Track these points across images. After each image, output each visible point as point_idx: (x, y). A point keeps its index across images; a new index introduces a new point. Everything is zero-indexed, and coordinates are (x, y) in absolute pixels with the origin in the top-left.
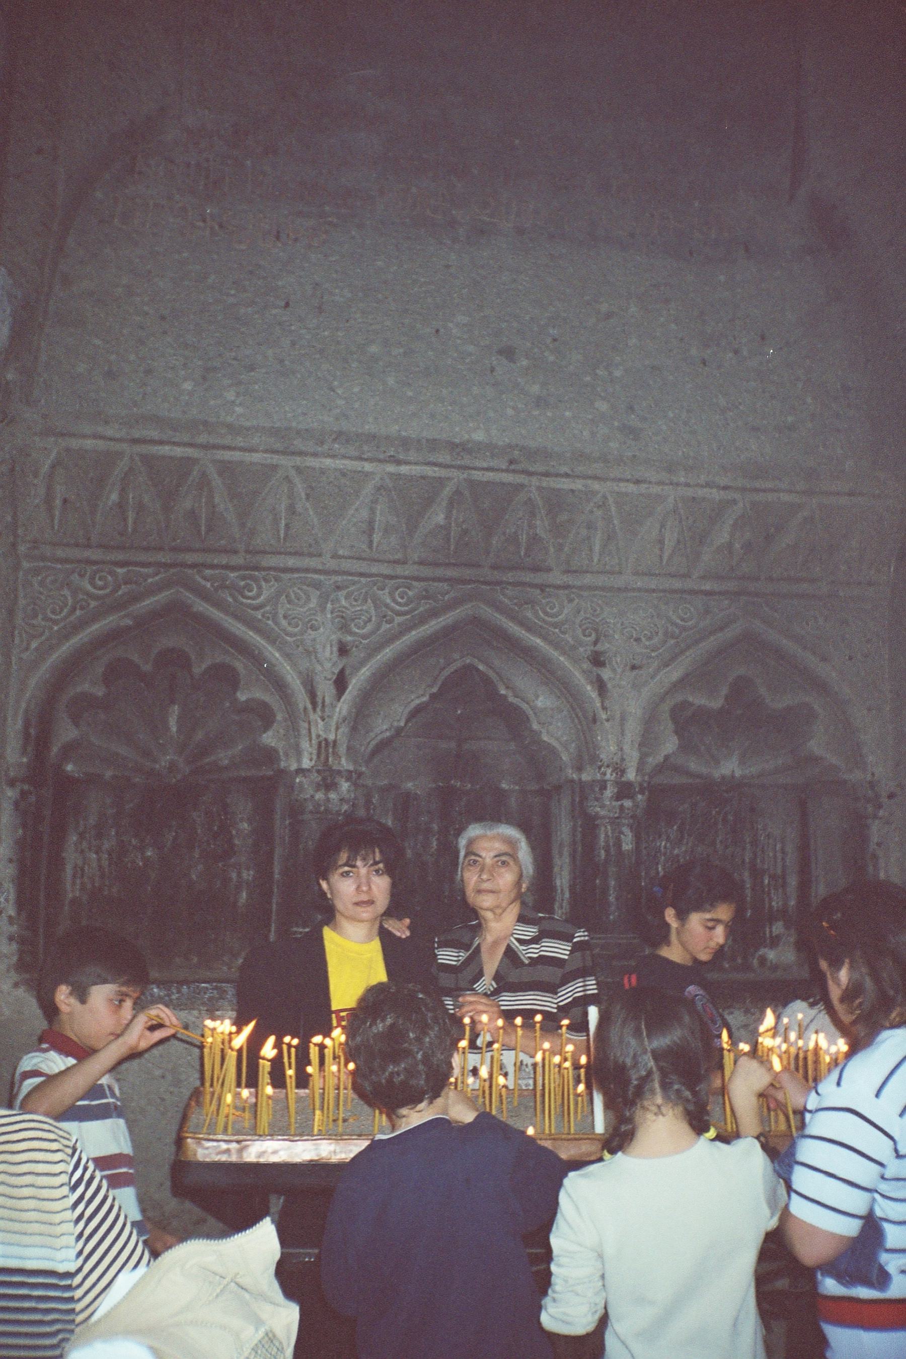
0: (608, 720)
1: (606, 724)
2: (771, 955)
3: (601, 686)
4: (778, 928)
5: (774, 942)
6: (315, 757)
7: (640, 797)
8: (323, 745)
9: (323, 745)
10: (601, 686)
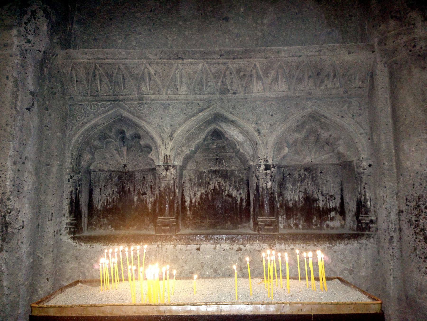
2: (331, 224)
4: (333, 214)
5: (332, 219)
7: (273, 169)
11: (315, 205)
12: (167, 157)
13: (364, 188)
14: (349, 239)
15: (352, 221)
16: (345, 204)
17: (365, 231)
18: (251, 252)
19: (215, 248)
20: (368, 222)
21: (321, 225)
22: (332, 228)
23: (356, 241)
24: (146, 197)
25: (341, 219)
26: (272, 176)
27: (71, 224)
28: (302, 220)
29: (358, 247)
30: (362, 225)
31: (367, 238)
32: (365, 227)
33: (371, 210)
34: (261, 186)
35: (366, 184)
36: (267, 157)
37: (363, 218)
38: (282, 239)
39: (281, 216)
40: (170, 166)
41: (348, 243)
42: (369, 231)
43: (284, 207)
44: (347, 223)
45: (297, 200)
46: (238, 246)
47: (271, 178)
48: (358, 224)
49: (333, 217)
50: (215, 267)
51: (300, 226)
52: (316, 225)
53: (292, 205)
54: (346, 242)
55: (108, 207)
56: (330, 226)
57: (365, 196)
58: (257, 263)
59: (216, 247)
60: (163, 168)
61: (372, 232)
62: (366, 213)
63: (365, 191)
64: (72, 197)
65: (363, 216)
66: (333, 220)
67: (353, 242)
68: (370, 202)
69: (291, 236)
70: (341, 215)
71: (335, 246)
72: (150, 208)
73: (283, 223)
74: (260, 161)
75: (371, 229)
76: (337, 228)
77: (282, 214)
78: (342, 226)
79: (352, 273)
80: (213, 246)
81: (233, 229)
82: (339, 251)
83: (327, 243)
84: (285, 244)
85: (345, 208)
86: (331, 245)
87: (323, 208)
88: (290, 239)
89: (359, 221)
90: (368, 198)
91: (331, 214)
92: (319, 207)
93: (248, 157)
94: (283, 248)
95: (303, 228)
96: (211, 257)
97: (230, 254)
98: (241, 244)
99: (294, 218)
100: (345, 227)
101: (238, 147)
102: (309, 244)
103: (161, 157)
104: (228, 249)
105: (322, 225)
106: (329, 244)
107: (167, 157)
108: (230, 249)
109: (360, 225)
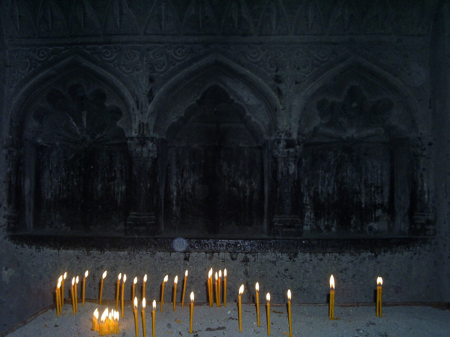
0: (283, 110)
1: (282, 111)
2: (375, 226)
3: (279, 92)
4: (379, 212)
5: (377, 220)
6: (137, 131)
7: (298, 147)
8: (142, 126)
9: (142, 126)
10: (279, 92)
12: (143, 126)
13: (422, 176)
24: (114, 184)
26: (296, 157)
27: (9, 218)
33: (429, 206)
34: (280, 171)
35: (424, 169)
36: (290, 129)
40: (147, 138)
45: (331, 192)
47: (294, 159)
49: (379, 217)
51: (333, 229)
52: (355, 228)
53: (323, 200)
55: (61, 196)
57: (423, 186)
60: (137, 141)
63: (422, 180)
64: (11, 181)
68: (429, 195)
72: (119, 201)
73: (310, 225)
74: (280, 134)
90: (425, 189)
91: (376, 213)
93: (263, 129)
101: (248, 114)
103: (135, 126)
107: (143, 126)
109: (413, 226)
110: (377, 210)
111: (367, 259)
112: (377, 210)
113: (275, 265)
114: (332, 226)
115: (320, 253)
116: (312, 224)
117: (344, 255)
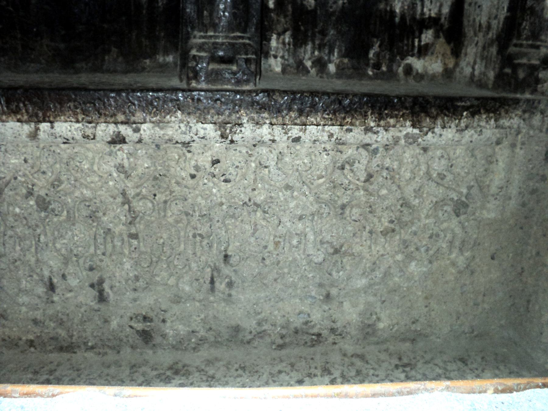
2: (418, 64)
4: (427, 36)
5: (423, 51)
11: (382, 6)
14: (474, 112)
15: (482, 58)
16: (466, 6)
17: (523, 92)
18: (158, 146)
19: (34, 136)
20: (535, 62)
21: (390, 69)
22: (420, 77)
23: (492, 122)
25: (449, 52)
28: (340, 51)
29: (494, 139)
30: (515, 71)
31: (524, 112)
32: (524, 79)
37: (524, 50)
38: (263, 107)
39: (279, 35)
41: (467, 127)
42: (534, 91)
43: (290, 8)
44: (463, 64)
46: (112, 128)
48: (502, 68)
49: (427, 45)
50: (42, 193)
51: (332, 68)
52: (377, 66)
54: (463, 125)
56: (414, 73)
58: (178, 183)
59: (37, 129)
61: (543, 93)
62: (535, 36)
65: (525, 42)
66: (426, 55)
67: (483, 123)
69: (293, 100)
70: (448, 42)
71: (430, 134)
73: (283, 57)
75: (539, 86)
76: (433, 77)
77: (280, 28)
78: (448, 73)
79: (462, 210)
80: (27, 128)
81: (126, 72)
82: (436, 148)
83: (408, 123)
84: (271, 124)
85: (465, 23)
86: (416, 131)
87: (403, 17)
88: (290, 109)
89: (507, 60)
91: (423, 36)
92: (392, 13)
94: (267, 138)
95: (341, 72)
96: (26, 161)
97: (90, 155)
98: (122, 123)
99: (317, 42)
100: (457, 74)
102: (352, 124)
104: (78, 136)
105: (395, 67)
106: (413, 126)
108: (85, 137)
109: (508, 70)
110: (424, 31)
111: (402, 142)
112: (424, 31)
113: (189, 152)
114: (330, 62)
115: (296, 124)
116: (286, 54)
117: (351, 130)
